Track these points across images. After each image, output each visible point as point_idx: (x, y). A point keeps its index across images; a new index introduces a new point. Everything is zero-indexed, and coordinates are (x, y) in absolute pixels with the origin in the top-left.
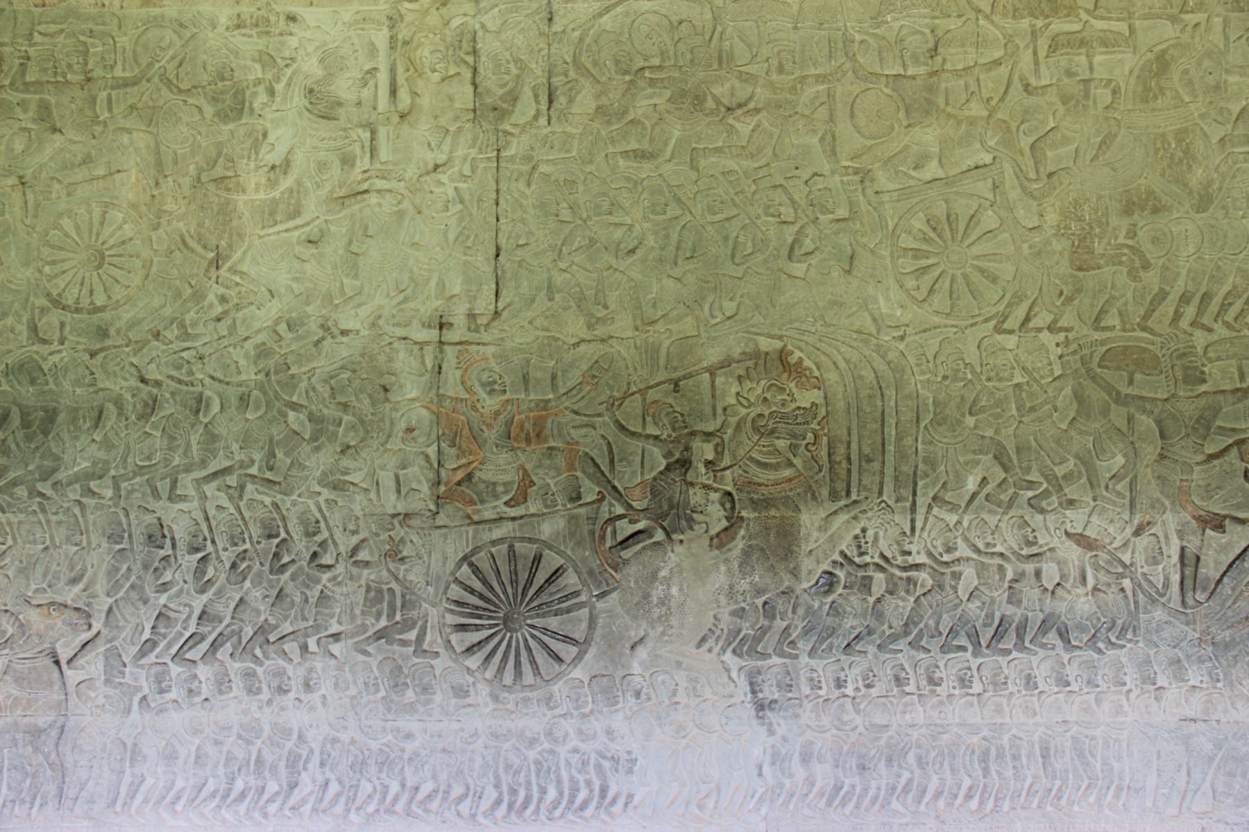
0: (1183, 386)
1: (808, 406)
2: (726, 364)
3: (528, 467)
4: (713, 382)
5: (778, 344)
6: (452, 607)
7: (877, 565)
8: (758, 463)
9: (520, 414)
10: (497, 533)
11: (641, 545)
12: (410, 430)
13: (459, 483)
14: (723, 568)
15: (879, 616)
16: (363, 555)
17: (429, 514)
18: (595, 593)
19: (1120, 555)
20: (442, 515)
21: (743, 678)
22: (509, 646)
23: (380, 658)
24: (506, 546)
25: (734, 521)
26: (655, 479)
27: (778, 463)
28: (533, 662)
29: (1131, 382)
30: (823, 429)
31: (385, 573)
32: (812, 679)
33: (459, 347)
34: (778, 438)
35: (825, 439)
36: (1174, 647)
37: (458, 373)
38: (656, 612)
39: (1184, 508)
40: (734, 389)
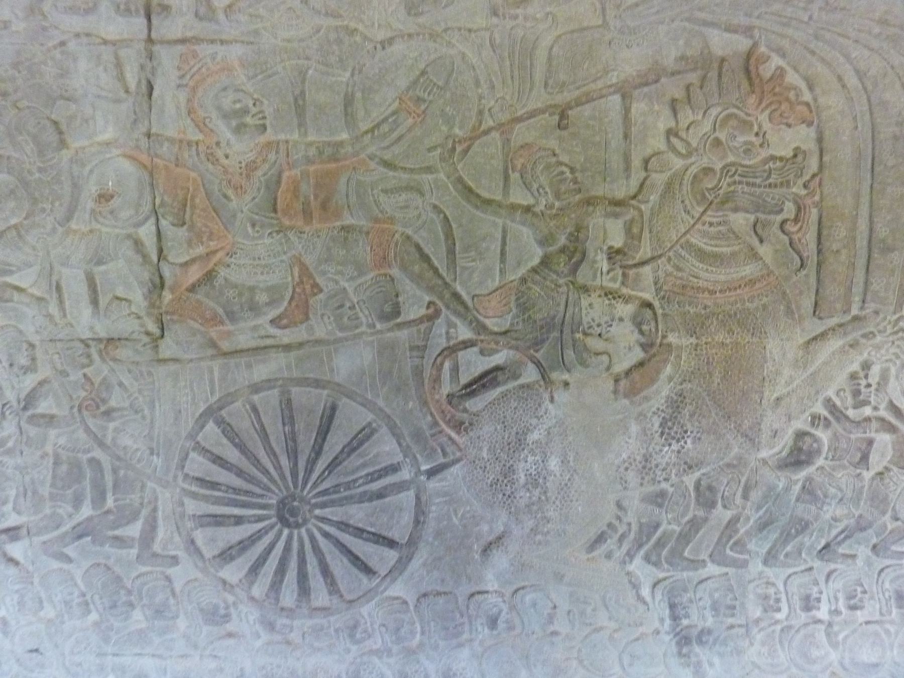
1: (788, 153)
2: (651, 77)
3: (309, 260)
4: (627, 110)
5: (743, 44)
6: (194, 488)
7: (882, 420)
8: (702, 255)
9: (291, 166)
10: (262, 371)
11: (499, 390)
12: (104, 197)
13: (192, 289)
14: (634, 428)
15: (880, 501)
16: (44, 406)
17: (146, 339)
18: (424, 467)
20: (168, 339)
21: (659, 596)
22: (287, 549)
23: (86, 564)
24: (276, 392)
25: (653, 350)
26: (523, 280)
27: (734, 254)
28: (326, 572)
30: (811, 194)
31: (81, 434)
32: (766, 597)
33: (180, 48)
34: (736, 210)
35: (814, 211)
37: (182, 97)
38: (523, 497)
40: (664, 122)
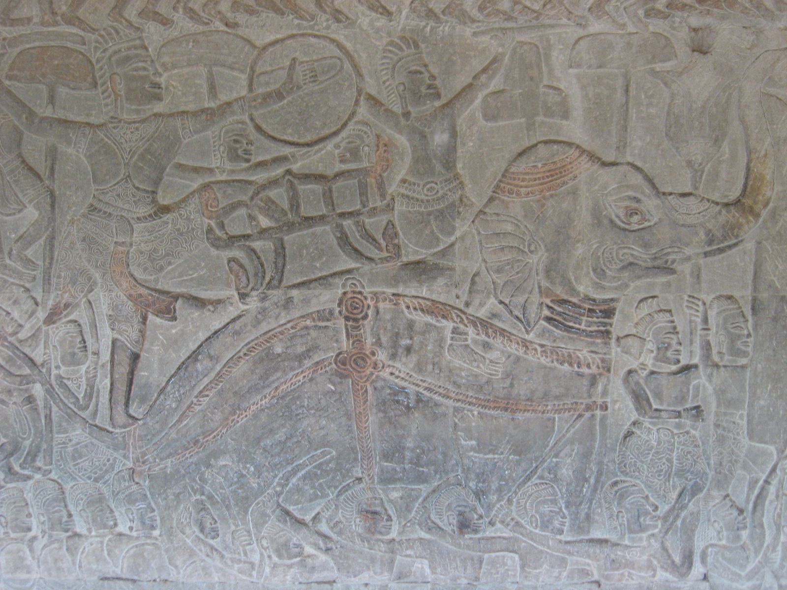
0: (126, 105)
19: (27, 350)
29: (52, 100)
36: (96, 480)
39: (118, 284)
